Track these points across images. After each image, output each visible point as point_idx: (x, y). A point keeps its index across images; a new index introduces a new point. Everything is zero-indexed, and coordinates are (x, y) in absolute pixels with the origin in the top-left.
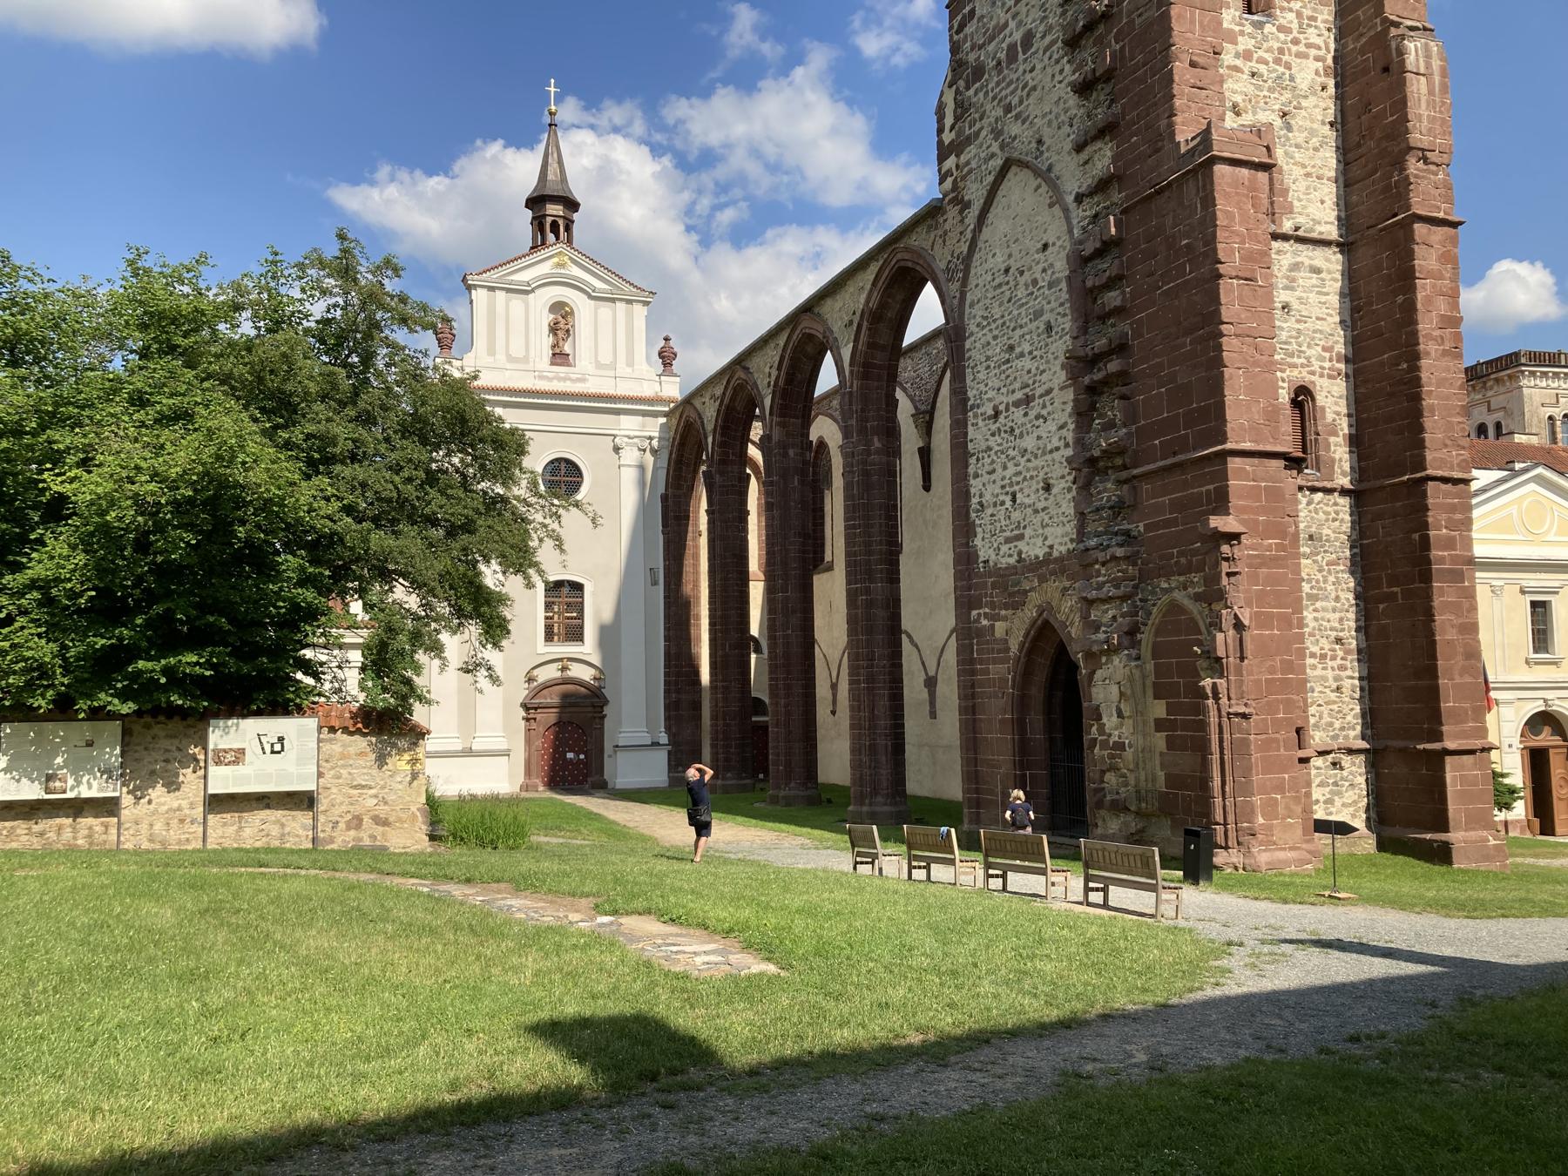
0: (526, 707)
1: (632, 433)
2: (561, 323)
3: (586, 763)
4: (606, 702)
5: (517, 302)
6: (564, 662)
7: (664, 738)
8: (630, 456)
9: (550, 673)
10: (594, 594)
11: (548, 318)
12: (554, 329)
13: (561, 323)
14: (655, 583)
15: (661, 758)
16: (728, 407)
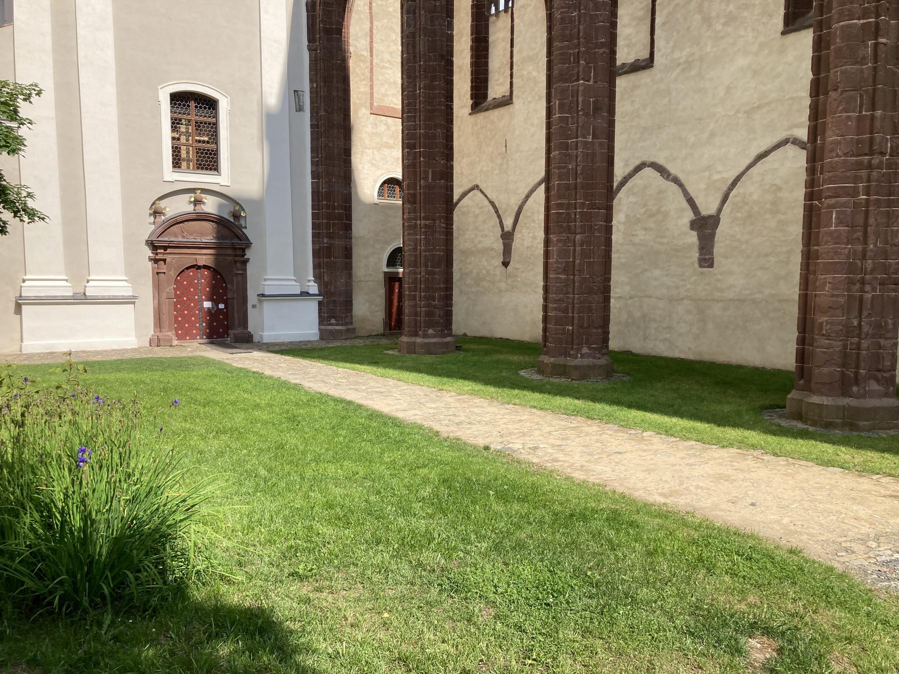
0: (153, 246)
3: (226, 313)
4: (248, 244)
6: (196, 193)
7: (314, 288)
9: (180, 206)
10: (231, 114)
14: (300, 109)
15: (310, 311)
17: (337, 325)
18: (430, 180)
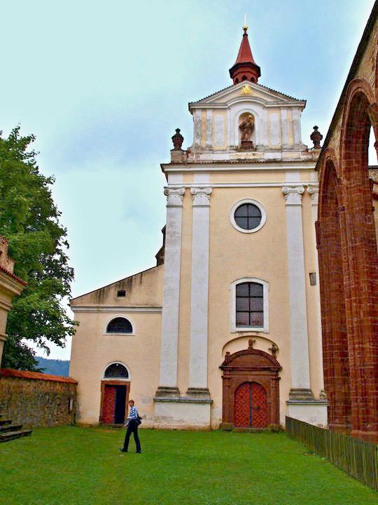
1: (293, 185)
2: (247, 126)
4: (279, 369)
5: (218, 117)
8: (294, 198)
11: (238, 124)
12: (242, 128)
13: (247, 126)
14: (313, 284)
16: (348, 123)
17: (340, 423)
18: (362, 317)
